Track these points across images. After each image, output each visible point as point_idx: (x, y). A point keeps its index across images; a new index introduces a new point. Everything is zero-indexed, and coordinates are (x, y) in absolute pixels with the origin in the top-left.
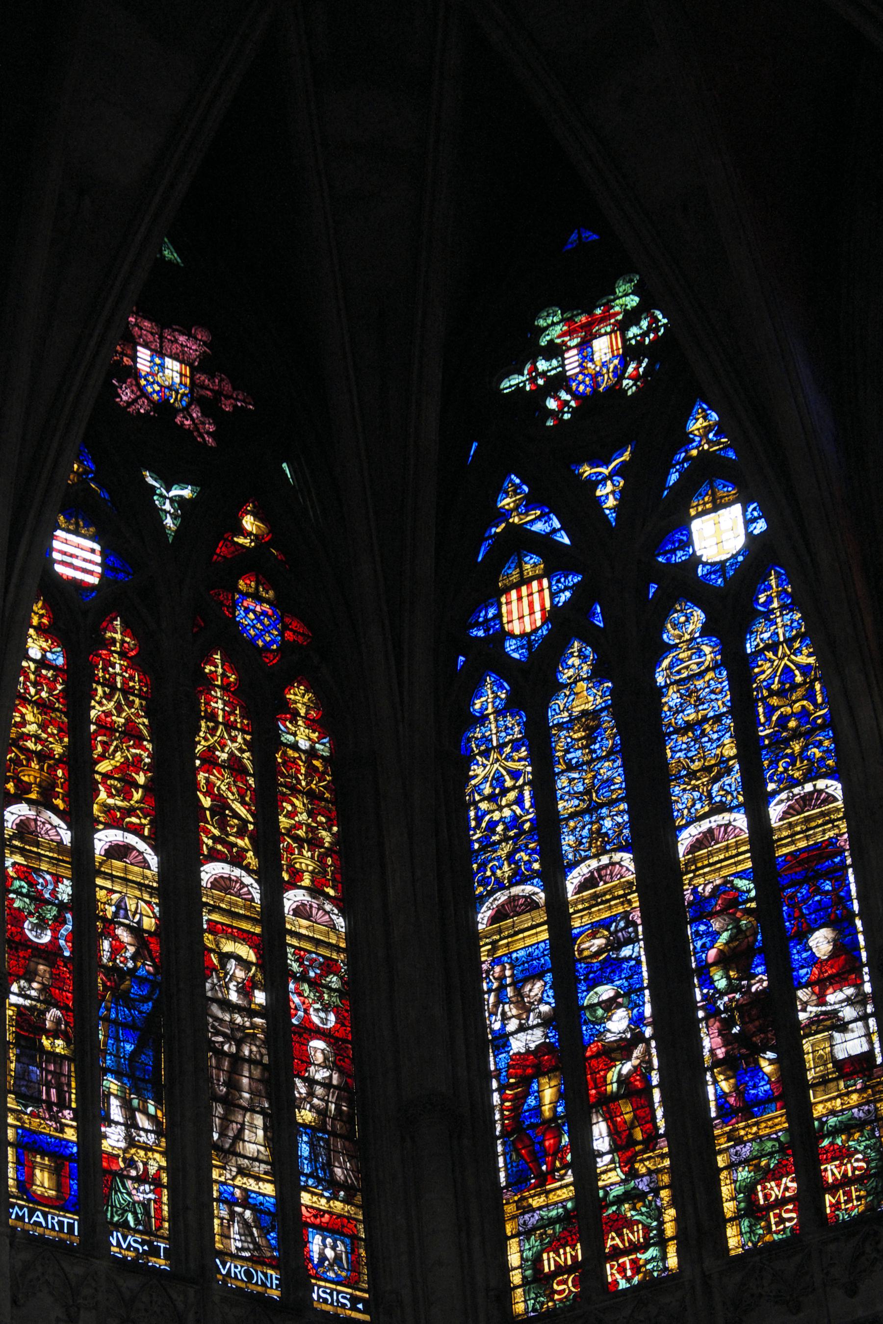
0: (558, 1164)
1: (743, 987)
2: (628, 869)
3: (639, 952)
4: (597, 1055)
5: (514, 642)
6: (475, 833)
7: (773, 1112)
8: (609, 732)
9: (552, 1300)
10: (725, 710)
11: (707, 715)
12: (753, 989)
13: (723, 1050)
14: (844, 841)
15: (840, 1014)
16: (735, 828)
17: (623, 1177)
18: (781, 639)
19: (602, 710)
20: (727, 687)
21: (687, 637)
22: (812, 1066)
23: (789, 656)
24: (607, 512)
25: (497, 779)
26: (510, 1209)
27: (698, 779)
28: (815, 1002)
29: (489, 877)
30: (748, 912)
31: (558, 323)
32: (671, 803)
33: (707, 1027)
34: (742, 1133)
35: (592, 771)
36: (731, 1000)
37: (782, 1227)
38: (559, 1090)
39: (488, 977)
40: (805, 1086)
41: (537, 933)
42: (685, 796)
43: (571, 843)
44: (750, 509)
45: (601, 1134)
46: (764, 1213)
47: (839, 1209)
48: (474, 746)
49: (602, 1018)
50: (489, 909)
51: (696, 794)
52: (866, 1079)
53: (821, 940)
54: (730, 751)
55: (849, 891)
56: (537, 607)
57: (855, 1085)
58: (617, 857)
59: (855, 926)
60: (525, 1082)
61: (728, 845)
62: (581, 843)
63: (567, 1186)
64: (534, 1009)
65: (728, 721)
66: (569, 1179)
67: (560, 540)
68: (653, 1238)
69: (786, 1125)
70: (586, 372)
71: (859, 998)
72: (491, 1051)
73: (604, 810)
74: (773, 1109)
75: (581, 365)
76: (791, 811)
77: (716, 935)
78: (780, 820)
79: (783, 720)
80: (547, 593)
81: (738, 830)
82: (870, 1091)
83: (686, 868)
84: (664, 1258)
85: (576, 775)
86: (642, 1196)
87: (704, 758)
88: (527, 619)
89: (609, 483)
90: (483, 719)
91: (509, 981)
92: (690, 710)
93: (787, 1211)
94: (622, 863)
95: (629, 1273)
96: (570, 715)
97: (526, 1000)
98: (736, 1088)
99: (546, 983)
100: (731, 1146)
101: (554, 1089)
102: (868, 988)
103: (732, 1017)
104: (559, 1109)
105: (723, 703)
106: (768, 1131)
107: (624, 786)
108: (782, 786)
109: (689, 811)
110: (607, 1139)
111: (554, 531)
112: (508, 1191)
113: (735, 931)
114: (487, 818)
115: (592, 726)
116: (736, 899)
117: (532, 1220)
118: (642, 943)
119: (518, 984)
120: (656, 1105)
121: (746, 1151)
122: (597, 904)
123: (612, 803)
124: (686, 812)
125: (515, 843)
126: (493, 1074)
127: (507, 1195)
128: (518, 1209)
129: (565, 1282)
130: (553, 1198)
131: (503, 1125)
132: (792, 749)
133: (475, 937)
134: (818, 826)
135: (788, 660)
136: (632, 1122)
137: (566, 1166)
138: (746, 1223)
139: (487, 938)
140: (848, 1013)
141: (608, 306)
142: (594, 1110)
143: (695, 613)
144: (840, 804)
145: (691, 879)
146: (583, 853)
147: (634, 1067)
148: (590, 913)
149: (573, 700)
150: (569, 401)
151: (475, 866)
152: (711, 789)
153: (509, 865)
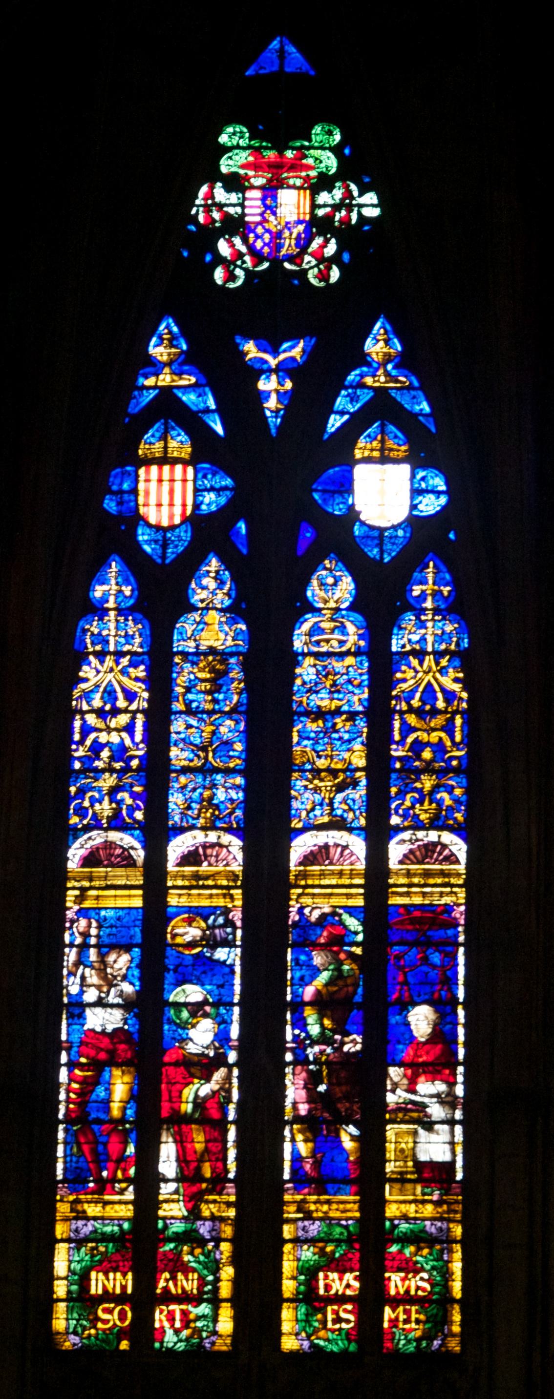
0: (119, 1174)
1: (335, 1041)
2: (234, 858)
3: (234, 960)
4: (176, 1064)
5: (148, 531)
6: (76, 750)
7: (346, 1195)
8: (235, 684)
9: (95, 1327)
10: (360, 709)
11: (341, 707)
12: (346, 1048)
13: (306, 1106)
14: (459, 913)
15: (428, 1110)
16: (352, 854)
17: (186, 1214)
18: (430, 649)
19: (232, 654)
20: (366, 683)
21: (332, 604)
22: (393, 1158)
23: (434, 673)
24: (268, 413)
25: (109, 693)
26: (63, 1209)
27: (322, 780)
28: (405, 1087)
29: (87, 809)
30: (351, 956)
31: (244, 149)
32: (290, 798)
33: (294, 1074)
34: (312, 1207)
35: (212, 724)
36: (322, 1052)
37: (337, 1326)
38: (131, 1090)
39: (71, 928)
40: (382, 1179)
41: (129, 896)
42: (307, 795)
43: (179, 802)
44: (419, 477)
45: (168, 1157)
46: (322, 1305)
47: (396, 1327)
48: (88, 641)
49: (187, 1023)
50: (82, 847)
51: (318, 798)
52: (443, 1192)
53: (422, 1018)
54: (359, 761)
55: (456, 973)
56: (178, 500)
57: (431, 1194)
58: (226, 838)
59: (456, 1015)
60: (98, 1067)
61: (342, 870)
62: (189, 808)
63: (126, 1203)
64: (116, 985)
65: (362, 724)
66: (130, 1195)
67: (212, 424)
68: (206, 1293)
69: (357, 1214)
70: (266, 225)
71: (449, 1099)
72: (64, 1016)
73: (219, 777)
74: (348, 1192)
75: (262, 214)
76: (412, 857)
77: (316, 971)
78: (401, 862)
79: (418, 747)
80: (190, 486)
81: (354, 858)
82: (445, 1207)
83: (296, 880)
84: (215, 1320)
85: (194, 723)
86: (201, 1242)
87: (332, 760)
88: (165, 509)
89: (274, 377)
90: (101, 612)
91: (93, 941)
92: (324, 694)
93: (345, 1311)
94: (230, 848)
95: (178, 1324)
96: (197, 647)
97: (109, 970)
98: (314, 1153)
99: (131, 961)
100: (299, 1219)
101: (127, 1087)
102: (460, 1091)
103: (320, 1071)
104: (129, 1112)
105: (360, 700)
106: (338, 1214)
107: (243, 756)
108: (406, 824)
109: (308, 815)
110: (174, 1165)
111: (207, 411)
112: (64, 1187)
113: (336, 973)
114: (93, 736)
115: (218, 670)
116: (342, 937)
117: (87, 1229)
118: (238, 951)
119: (104, 948)
120: (230, 1144)
121: (314, 1229)
122: (198, 887)
123: (228, 772)
124: (304, 814)
125: (120, 779)
126: (65, 1045)
127: (62, 1191)
128: (72, 1210)
129: (110, 1311)
130: (110, 1211)
131: (67, 1108)
132: (422, 784)
133: (63, 875)
134: (435, 885)
135: (434, 677)
136: (202, 1155)
137: (127, 1179)
138: (303, 1309)
139: (76, 881)
140: (436, 1111)
141: (301, 154)
142: (165, 1127)
143: (344, 578)
144: (461, 868)
145: (299, 896)
146: (191, 821)
147: (212, 1091)
148: (189, 895)
149: (202, 630)
150: (244, 255)
151: (73, 789)
152: (334, 798)
153: (111, 802)
